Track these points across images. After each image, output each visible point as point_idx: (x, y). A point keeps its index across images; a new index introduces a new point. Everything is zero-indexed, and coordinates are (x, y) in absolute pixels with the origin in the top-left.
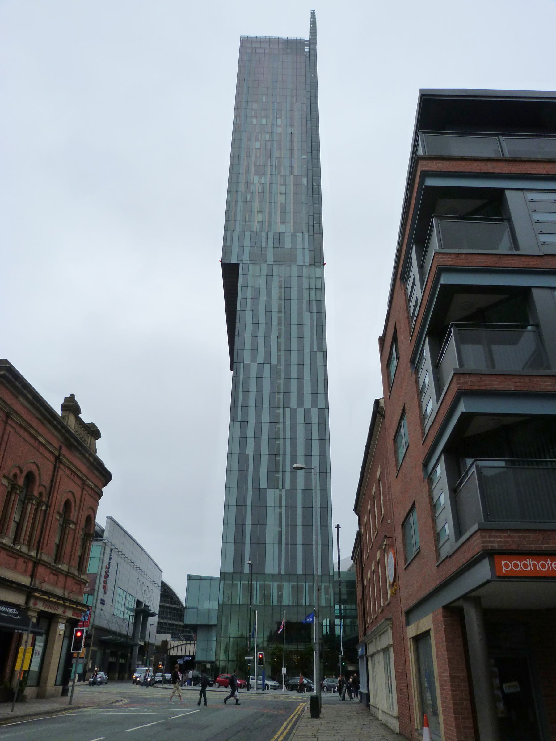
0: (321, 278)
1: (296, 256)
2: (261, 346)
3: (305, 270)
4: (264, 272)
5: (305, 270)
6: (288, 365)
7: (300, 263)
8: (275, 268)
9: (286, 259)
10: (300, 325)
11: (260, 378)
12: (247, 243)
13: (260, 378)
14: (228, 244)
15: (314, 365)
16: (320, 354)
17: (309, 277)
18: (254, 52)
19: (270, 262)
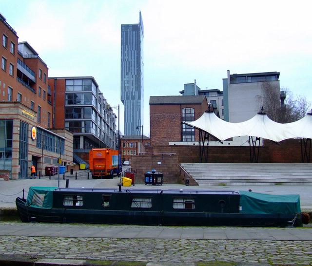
0: (140, 103)
4: (129, 102)
6: (134, 122)
9: (133, 98)
11: (129, 126)
12: (125, 95)
13: (129, 126)
15: (138, 123)
18: (125, 29)
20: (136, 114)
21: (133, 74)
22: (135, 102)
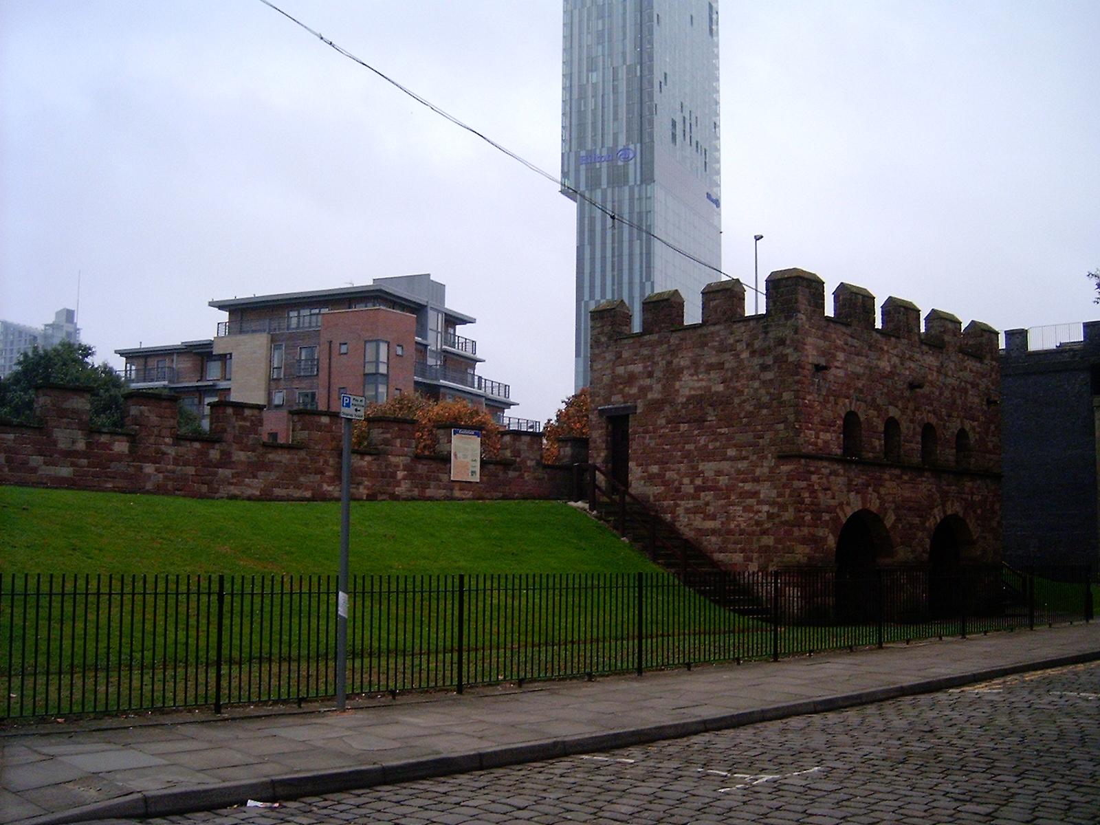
1: (626, 175)
2: (598, 282)
3: (636, 189)
5: (636, 189)
7: (631, 183)
8: (609, 191)
9: (618, 179)
10: (631, 255)
14: (566, 170)
16: (648, 284)
17: (640, 199)
19: (604, 186)
20: (631, 255)
21: (618, 61)
22: (627, 197)
